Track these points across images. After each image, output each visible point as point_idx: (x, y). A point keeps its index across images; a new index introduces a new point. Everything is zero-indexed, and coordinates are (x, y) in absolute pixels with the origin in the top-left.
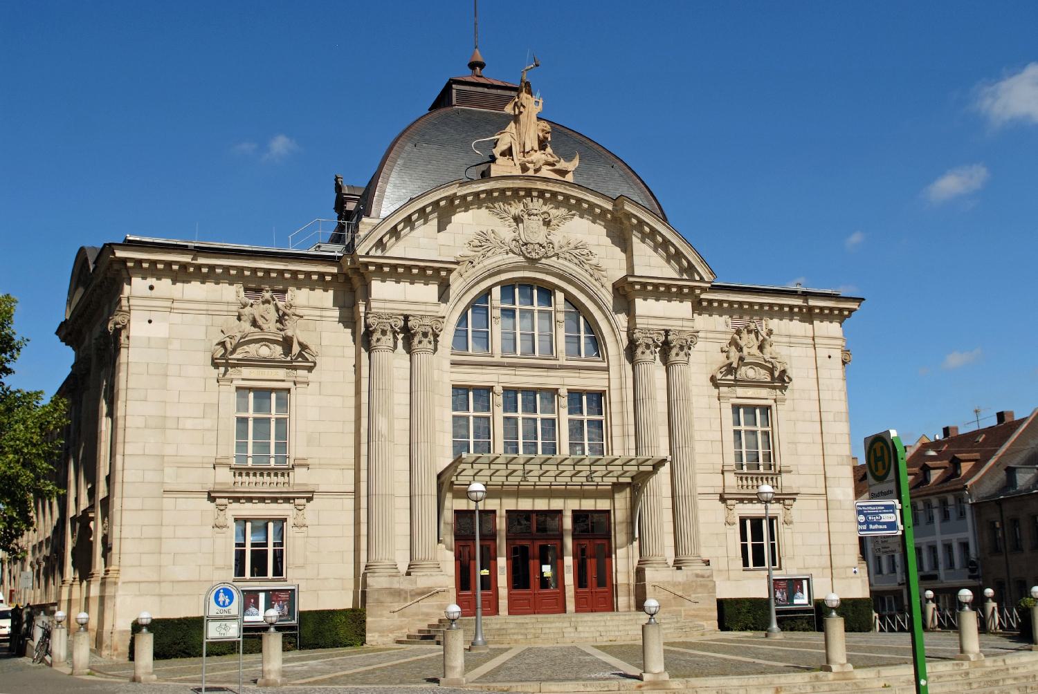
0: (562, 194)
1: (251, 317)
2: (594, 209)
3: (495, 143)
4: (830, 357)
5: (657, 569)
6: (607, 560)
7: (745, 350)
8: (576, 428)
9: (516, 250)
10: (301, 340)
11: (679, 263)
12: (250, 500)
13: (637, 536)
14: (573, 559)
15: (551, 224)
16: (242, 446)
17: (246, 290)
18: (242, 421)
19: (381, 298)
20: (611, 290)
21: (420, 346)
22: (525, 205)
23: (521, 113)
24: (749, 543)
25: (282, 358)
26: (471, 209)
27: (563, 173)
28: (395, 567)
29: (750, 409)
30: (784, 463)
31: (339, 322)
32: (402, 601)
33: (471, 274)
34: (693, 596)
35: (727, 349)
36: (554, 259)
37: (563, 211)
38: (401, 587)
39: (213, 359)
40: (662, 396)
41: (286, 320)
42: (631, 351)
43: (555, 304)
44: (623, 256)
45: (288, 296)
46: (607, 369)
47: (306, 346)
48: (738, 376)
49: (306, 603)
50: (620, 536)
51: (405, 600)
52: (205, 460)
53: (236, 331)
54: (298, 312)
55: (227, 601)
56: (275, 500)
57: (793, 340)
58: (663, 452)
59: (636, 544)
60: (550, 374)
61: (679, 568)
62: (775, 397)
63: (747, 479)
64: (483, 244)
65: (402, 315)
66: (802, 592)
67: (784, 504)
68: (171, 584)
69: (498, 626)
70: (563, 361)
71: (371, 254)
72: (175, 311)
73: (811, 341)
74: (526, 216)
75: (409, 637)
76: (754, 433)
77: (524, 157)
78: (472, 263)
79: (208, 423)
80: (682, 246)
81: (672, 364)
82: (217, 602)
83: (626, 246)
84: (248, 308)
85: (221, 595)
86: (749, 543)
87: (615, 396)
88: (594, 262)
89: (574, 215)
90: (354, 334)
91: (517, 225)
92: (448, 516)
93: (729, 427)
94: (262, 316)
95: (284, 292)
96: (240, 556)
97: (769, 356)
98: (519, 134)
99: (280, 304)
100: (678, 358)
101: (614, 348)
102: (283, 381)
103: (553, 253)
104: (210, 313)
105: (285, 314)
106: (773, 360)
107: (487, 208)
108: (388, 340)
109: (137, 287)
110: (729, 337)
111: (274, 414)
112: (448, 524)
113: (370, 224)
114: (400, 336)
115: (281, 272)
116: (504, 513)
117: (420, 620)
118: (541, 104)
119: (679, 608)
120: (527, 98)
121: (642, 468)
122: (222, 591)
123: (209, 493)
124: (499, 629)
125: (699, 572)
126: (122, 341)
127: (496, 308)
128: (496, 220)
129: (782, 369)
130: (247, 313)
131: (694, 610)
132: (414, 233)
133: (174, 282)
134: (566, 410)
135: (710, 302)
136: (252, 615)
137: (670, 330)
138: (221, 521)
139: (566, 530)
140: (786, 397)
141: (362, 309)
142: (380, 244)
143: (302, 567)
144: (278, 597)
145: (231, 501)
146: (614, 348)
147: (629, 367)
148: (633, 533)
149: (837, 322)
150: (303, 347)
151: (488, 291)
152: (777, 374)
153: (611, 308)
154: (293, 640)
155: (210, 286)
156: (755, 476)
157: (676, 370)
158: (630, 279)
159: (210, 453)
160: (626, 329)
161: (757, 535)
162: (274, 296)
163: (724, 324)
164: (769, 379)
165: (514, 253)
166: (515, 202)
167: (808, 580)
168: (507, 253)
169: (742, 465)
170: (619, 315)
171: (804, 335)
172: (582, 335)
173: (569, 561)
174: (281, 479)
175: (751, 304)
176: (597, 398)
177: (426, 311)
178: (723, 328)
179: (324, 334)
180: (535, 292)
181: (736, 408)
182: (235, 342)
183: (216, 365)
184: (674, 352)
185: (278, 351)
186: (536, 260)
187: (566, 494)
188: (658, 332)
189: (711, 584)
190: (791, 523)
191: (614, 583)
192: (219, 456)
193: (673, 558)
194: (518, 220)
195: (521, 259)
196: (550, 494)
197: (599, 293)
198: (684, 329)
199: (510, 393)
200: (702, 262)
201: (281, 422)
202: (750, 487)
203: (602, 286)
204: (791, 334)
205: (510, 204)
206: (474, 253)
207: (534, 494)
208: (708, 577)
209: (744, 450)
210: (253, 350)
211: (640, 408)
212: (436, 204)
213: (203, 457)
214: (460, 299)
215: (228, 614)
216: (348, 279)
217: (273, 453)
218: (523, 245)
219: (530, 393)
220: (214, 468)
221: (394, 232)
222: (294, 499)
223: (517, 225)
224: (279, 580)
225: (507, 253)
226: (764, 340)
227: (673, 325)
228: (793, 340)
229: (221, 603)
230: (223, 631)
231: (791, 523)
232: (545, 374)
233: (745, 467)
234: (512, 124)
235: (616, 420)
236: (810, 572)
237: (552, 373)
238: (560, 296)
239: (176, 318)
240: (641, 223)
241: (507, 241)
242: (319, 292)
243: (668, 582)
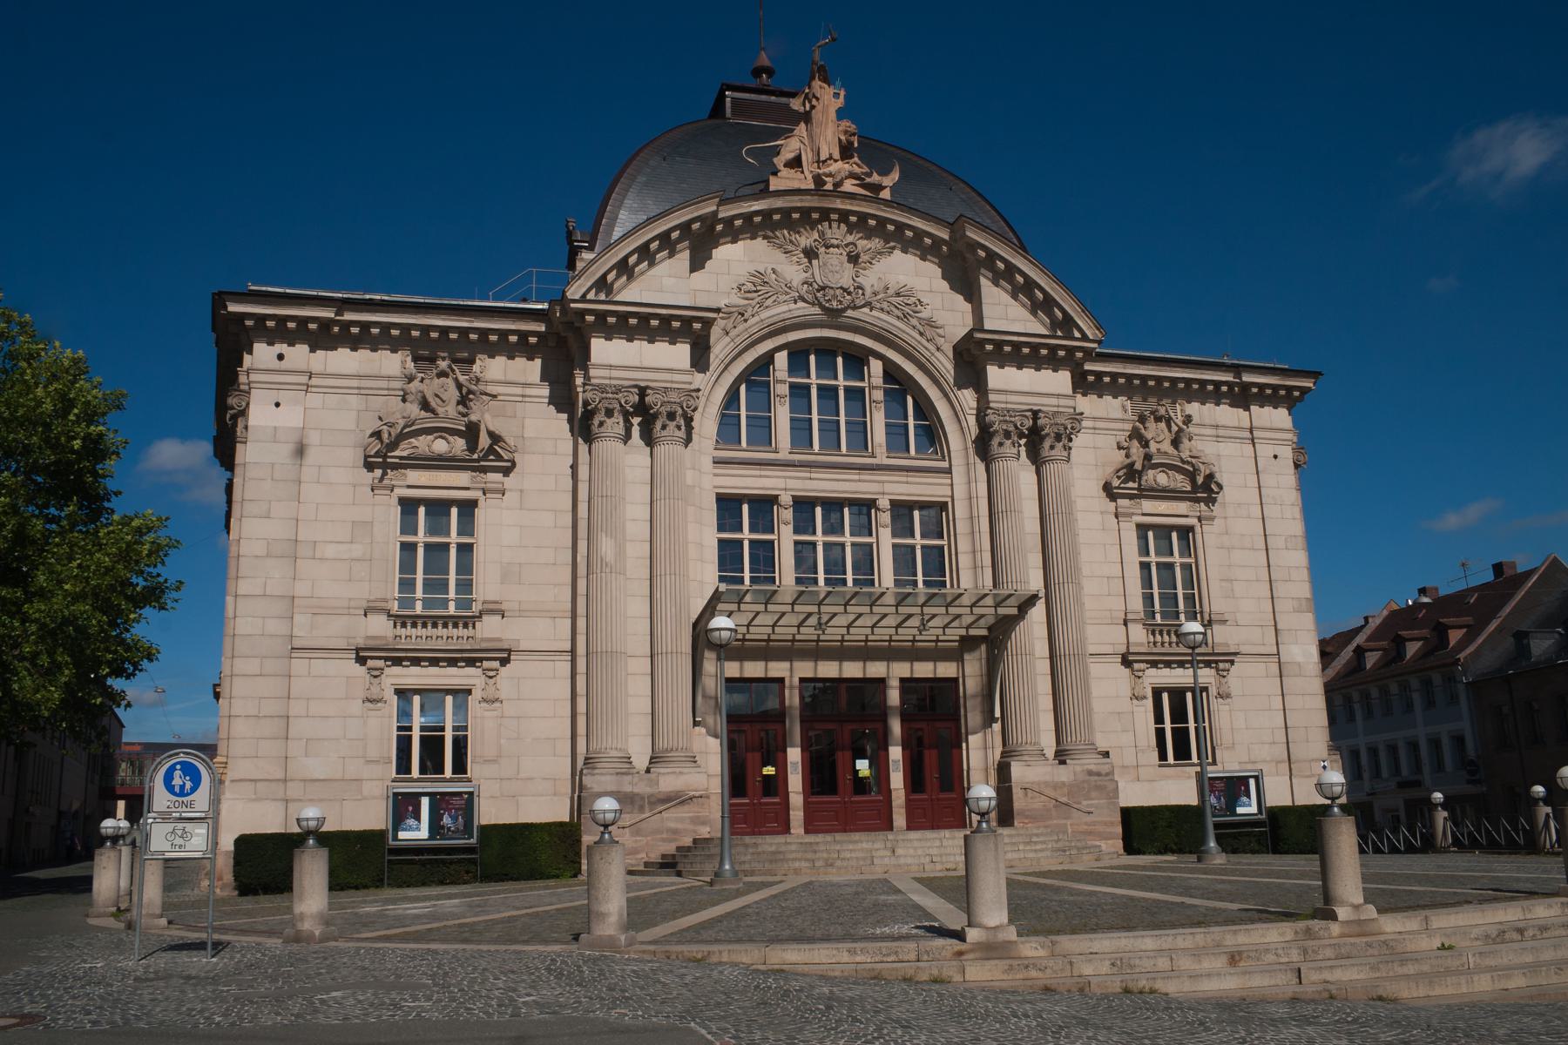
0: (873, 216)
2: (922, 240)
3: (776, 151)
5: (1029, 763)
6: (954, 751)
7: (1153, 447)
8: (904, 558)
9: (809, 297)
10: (491, 428)
11: (1050, 315)
12: (416, 662)
13: (998, 714)
14: (903, 749)
15: (860, 260)
16: (407, 585)
17: (415, 359)
19: (606, 362)
20: (951, 355)
21: (664, 433)
22: (822, 234)
23: (813, 107)
24: (1168, 726)
25: (466, 455)
26: (741, 240)
27: (878, 188)
28: (628, 760)
29: (1163, 532)
31: (549, 404)
32: (636, 811)
33: (743, 331)
34: (1085, 803)
35: (1126, 445)
36: (866, 310)
37: (876, 243)
38: (636, 790)
39: (366, 457)
40: (1030, 510)
41: (471, 400)
42: (983, 446)
43: (869, 376)
44: (968, 307)
45: (476, 368)
46: (949, 471)
47: (500, 437)
48: (1143, 483)
49: (490, 813)
50: (973, 717)
51: (641, 809)
52: (353, 604)
53: (399, 416)
54: (491, 389)
55: (188, 785)
56: (453, 662)
57: (1221, 432)
58: (1035, 583)
59: (997, 727)
60: (862, 477)
61: (1063, 762)
63: (1161, 633)
64: (759, 288)
65: (635, 386)
66: (1249, 796)
67: (1217, 670)
68: (302, 784)
69: (773, 848)
70: (882, 458)
71: (589, 297)
72: (314, 390)
73: (1247, 434)
74: (822, 250)
75: (646, 864)
76: (1170, 566)
77: (819, 168)
78: (743, 315)
79: (357, 550)
80: (1052, 288)
81: (1044, 462)
82: (169, 787)
83: (971, 294)
84: (416, 383)
85: (178, 773)
86: (1168, 726)
87: (961, 511)
88: (924, 315)
89: (893, 248)
90: (570, 421)
91: (810, 263)
92: (710, 683)
93: (1133, 557)
94: (437, 396)
95: (472, 362)
96: (404, 745)
97: (1188, 453)
98: (811, 136)
99: (462, 378)
100: (1053, 452)
101: (958, 441)
102: (468, 489)
103: (863, 302)
104: (363, 392)
105: (470, 392)
106: (1194, 461)
107: (765, 237)
108: (615, 425)
109: (262, 354)
110: (1129, 426)
111: (454, 538)
112: (711, 698)
114: (636, 421)
115: (464, 332)
116: (796, 681)
117: (664, 840)
118: (842, 96)
119: (1064, 821)
120: (821, 87)
121: (1001, 611)
122: (178, 767)
123: (358, 650)
124: (774, 853)
125: (1092, 767)
126: (239, 434)
127: (783, 382)
128: (778, 255)
129: (1208, 472)
130: (414, 391)
131: (1086, 824)
132: (656, 270)
133: (313, 350)
134: (889, 530)
135: (1099, 375)
136: (410, 829)
137: (1040, 411)
138: (375, 691)
139: (891, 707)
140: (1214, 514)
141: (579, 381)
142: (602, 284)
143: (494, 761)
144: (448, 803)
145: (389, 663)
146: (958, 441)
147: (981, 467)
148: (992, 711)
149: (1284, 407)
150: (495, 438)
151: (768, 359)
152: (1200, 480)
153: (952, 381)
154: (472, 868)
155: (364, 354)
157: (1050, 469)
158: (979, 335)
159: (363, 592)
160: (975, 412)
161: (1179, 714)
163: (1121, 409)
164: (1189, 488)
165: (804, 300)
166: (806, 229)
167: (1256, 778)
168: (795, 302)
169: (1154, 613)
170: (965, 391)
171: (1237, 425)
172: (911, 422)
173: (896, 753)
174: (461, 631)
175: (1159, 380)
176: (938, 510)
177: (672, 382)
178: (1119, 414)
179: (527, 422)
180: (840, 360)
181: (1142, 529)
183: (370, 467)
184: (1047, 444)
185: (460, 444)
186: (838, 313)
187: (890, 653)
188: (1022, 413)
189: (1111, 786)
190: (1228, 696)
191: (966, 785)
192: (372, 598)
193: (1054, 749)
194: (810, 254)
195: (817, 310)
196: (866, 653)
197: (933, 359)
198: (1061, 410)
199: (804, 506)
200: (1083, 311)
201: (466, 550)
202: (1166, 645)
203: (938, 349)
204: (1220, 424)
205: (799, 232)
206: (746, 302)
207: (842, 652)
208: (1107, 774)
209: (1156, 591)
210: (422, 444)
211: (1003, 526)
212: (685, 227)
213: (350, 599)
214: (726, 368)
215: (189, 809)
216: (562, 342)
217: (452, 594)
218: (818, 291)
219: (833, 506)
220: (365, 615)
221: (623, 267)
222: (481, 660)
223: (810, 263)
224: (460, 780)
225: (795, 302)
226: (1180, 430)
227: (1047, 404)
228: (1221, 432)
229: (177, 790)
230: (179, 841)
231: (1228, 696)
232: (857, 477)
233: (1158, 616)
234: (803, 125)
235: (964, 545)
236: (1259, 767)
237: (866, 476)
238: (876, 367)
239: (314, 399)
240: (992, 256)
241: (795, 284)
242: (520, 362)
243: (1045, 782)
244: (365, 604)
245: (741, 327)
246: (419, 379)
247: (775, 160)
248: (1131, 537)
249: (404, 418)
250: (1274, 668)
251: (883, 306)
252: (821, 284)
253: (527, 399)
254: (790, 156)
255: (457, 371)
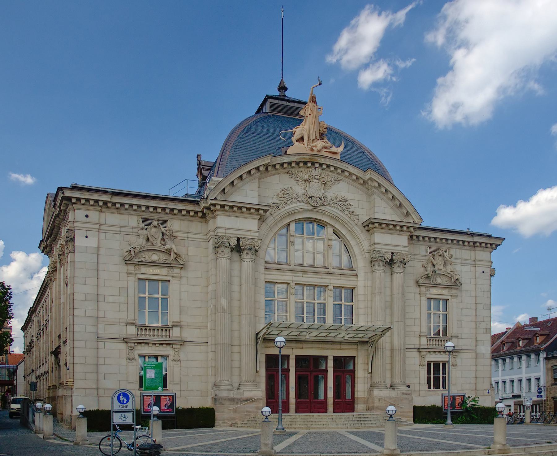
1: (146, 236)
4: (483, 272)
7: (437, 267)
10: (176, 251)
18: (142, 299)
19: (224, 226)
30: (455, 331)
36: (328, 207)
52: (121, 321)
60: (323, 277)
62: (451, 294)
64: (285, 196)
79: (122, 299)
101: (361, 264)
103: (327, 204)
106: (452, 273)
111: (160, 296)
113: (217, 181)
138: (131, 356)
156: (437, 339)
162: (160, 224)
165: (303, 202)
177: (250, 236)
179: (189, 248)
182: (136, 251)
190: (456, 365)
192: (128, 319)
201: (165, 300)
202: (434, 345)
206: (280, 202)
209: (432, 324)
232: (320, 277)
241: (299, 195)
244: (125, 321)
245: (277, 213)
246: (145, 229)
248: (424, 302)
249: (139, 245)
250: (474, 355)
251: (335, 206)
252: (310, 195)
253: (189, 239)
254: (299, 137)
255: (161, 226)
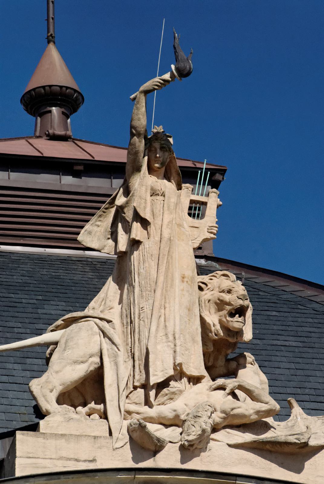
23: (135, 244)
77: (147, 403)
118: (211, 212)
247: (35, 385)
